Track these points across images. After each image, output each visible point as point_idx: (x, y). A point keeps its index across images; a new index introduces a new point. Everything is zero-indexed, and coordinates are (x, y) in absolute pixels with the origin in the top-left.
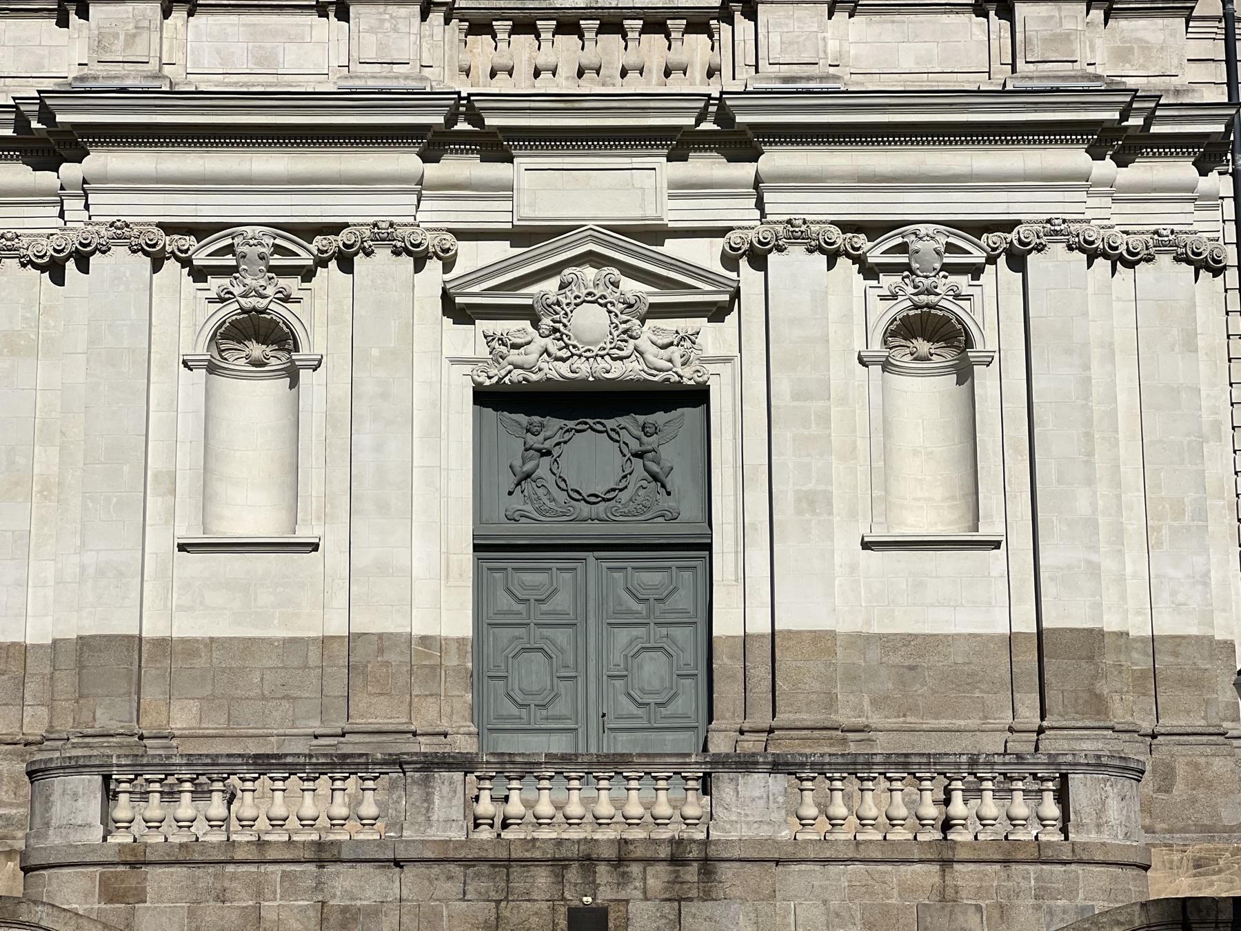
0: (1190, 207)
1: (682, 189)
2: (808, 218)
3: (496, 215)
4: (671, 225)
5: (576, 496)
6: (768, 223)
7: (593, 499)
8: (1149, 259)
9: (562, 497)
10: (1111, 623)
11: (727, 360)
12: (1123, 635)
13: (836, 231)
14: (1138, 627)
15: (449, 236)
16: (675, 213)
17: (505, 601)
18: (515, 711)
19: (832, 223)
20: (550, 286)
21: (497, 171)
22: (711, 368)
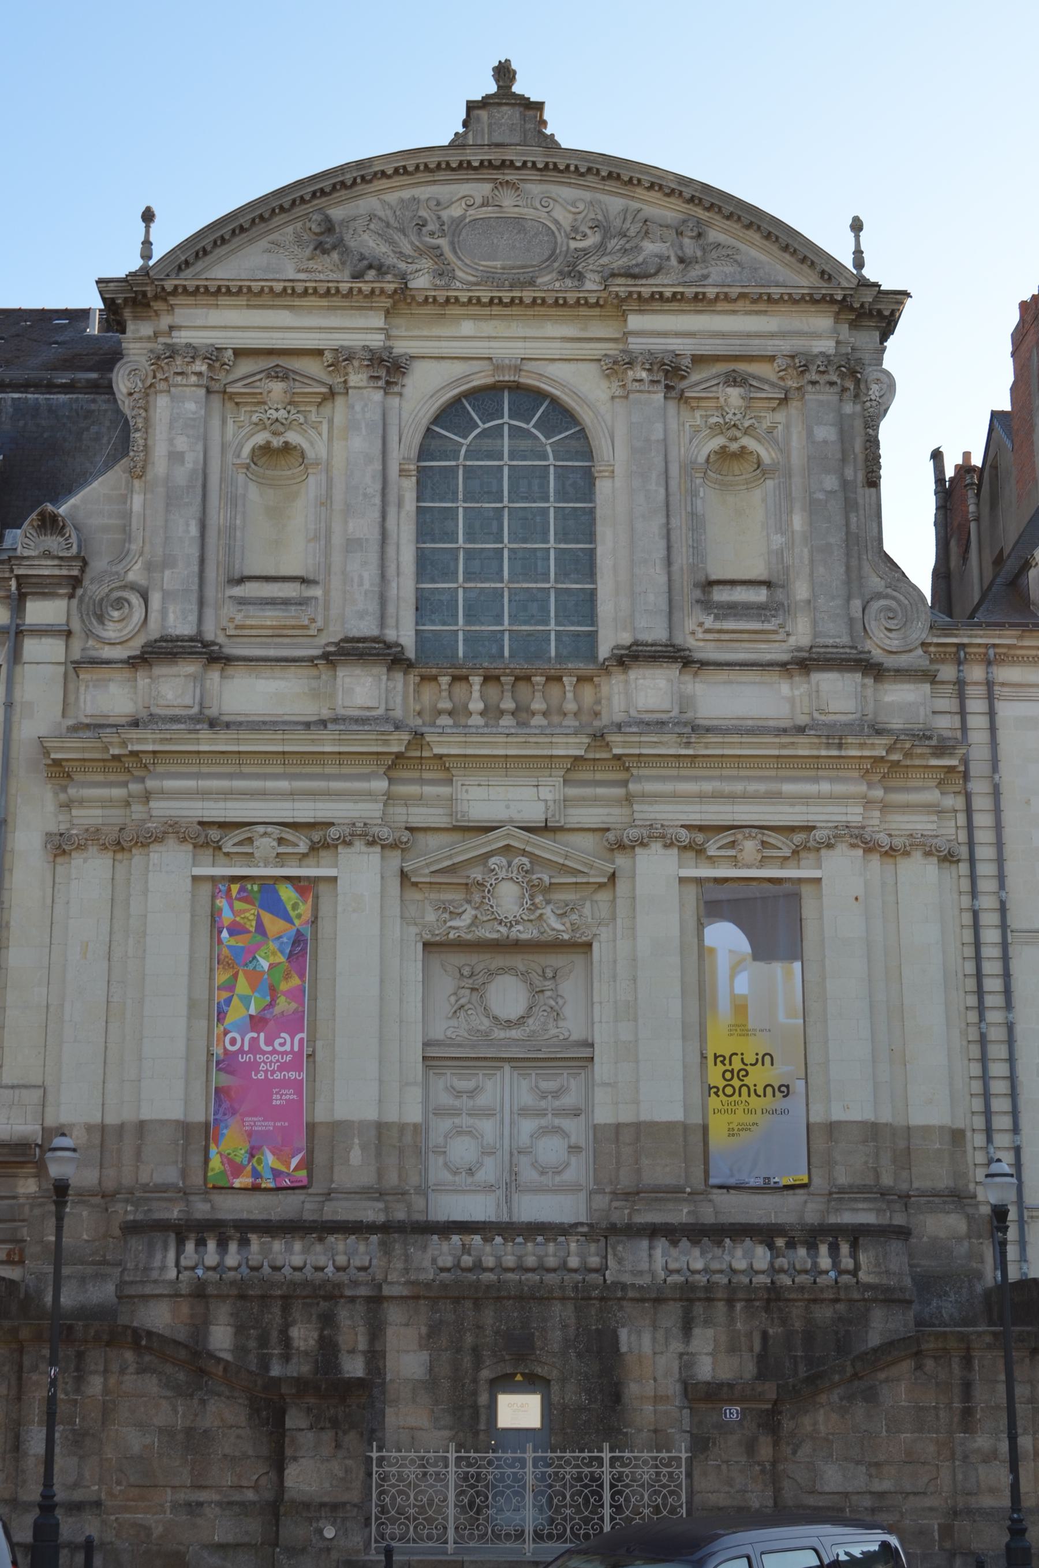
2: (666, 823)
6: (636, 826)
7: (509, 1024)
9: (486, 1022)
13: (683, 831)
18: (448, 1177)
19: (682, 826)
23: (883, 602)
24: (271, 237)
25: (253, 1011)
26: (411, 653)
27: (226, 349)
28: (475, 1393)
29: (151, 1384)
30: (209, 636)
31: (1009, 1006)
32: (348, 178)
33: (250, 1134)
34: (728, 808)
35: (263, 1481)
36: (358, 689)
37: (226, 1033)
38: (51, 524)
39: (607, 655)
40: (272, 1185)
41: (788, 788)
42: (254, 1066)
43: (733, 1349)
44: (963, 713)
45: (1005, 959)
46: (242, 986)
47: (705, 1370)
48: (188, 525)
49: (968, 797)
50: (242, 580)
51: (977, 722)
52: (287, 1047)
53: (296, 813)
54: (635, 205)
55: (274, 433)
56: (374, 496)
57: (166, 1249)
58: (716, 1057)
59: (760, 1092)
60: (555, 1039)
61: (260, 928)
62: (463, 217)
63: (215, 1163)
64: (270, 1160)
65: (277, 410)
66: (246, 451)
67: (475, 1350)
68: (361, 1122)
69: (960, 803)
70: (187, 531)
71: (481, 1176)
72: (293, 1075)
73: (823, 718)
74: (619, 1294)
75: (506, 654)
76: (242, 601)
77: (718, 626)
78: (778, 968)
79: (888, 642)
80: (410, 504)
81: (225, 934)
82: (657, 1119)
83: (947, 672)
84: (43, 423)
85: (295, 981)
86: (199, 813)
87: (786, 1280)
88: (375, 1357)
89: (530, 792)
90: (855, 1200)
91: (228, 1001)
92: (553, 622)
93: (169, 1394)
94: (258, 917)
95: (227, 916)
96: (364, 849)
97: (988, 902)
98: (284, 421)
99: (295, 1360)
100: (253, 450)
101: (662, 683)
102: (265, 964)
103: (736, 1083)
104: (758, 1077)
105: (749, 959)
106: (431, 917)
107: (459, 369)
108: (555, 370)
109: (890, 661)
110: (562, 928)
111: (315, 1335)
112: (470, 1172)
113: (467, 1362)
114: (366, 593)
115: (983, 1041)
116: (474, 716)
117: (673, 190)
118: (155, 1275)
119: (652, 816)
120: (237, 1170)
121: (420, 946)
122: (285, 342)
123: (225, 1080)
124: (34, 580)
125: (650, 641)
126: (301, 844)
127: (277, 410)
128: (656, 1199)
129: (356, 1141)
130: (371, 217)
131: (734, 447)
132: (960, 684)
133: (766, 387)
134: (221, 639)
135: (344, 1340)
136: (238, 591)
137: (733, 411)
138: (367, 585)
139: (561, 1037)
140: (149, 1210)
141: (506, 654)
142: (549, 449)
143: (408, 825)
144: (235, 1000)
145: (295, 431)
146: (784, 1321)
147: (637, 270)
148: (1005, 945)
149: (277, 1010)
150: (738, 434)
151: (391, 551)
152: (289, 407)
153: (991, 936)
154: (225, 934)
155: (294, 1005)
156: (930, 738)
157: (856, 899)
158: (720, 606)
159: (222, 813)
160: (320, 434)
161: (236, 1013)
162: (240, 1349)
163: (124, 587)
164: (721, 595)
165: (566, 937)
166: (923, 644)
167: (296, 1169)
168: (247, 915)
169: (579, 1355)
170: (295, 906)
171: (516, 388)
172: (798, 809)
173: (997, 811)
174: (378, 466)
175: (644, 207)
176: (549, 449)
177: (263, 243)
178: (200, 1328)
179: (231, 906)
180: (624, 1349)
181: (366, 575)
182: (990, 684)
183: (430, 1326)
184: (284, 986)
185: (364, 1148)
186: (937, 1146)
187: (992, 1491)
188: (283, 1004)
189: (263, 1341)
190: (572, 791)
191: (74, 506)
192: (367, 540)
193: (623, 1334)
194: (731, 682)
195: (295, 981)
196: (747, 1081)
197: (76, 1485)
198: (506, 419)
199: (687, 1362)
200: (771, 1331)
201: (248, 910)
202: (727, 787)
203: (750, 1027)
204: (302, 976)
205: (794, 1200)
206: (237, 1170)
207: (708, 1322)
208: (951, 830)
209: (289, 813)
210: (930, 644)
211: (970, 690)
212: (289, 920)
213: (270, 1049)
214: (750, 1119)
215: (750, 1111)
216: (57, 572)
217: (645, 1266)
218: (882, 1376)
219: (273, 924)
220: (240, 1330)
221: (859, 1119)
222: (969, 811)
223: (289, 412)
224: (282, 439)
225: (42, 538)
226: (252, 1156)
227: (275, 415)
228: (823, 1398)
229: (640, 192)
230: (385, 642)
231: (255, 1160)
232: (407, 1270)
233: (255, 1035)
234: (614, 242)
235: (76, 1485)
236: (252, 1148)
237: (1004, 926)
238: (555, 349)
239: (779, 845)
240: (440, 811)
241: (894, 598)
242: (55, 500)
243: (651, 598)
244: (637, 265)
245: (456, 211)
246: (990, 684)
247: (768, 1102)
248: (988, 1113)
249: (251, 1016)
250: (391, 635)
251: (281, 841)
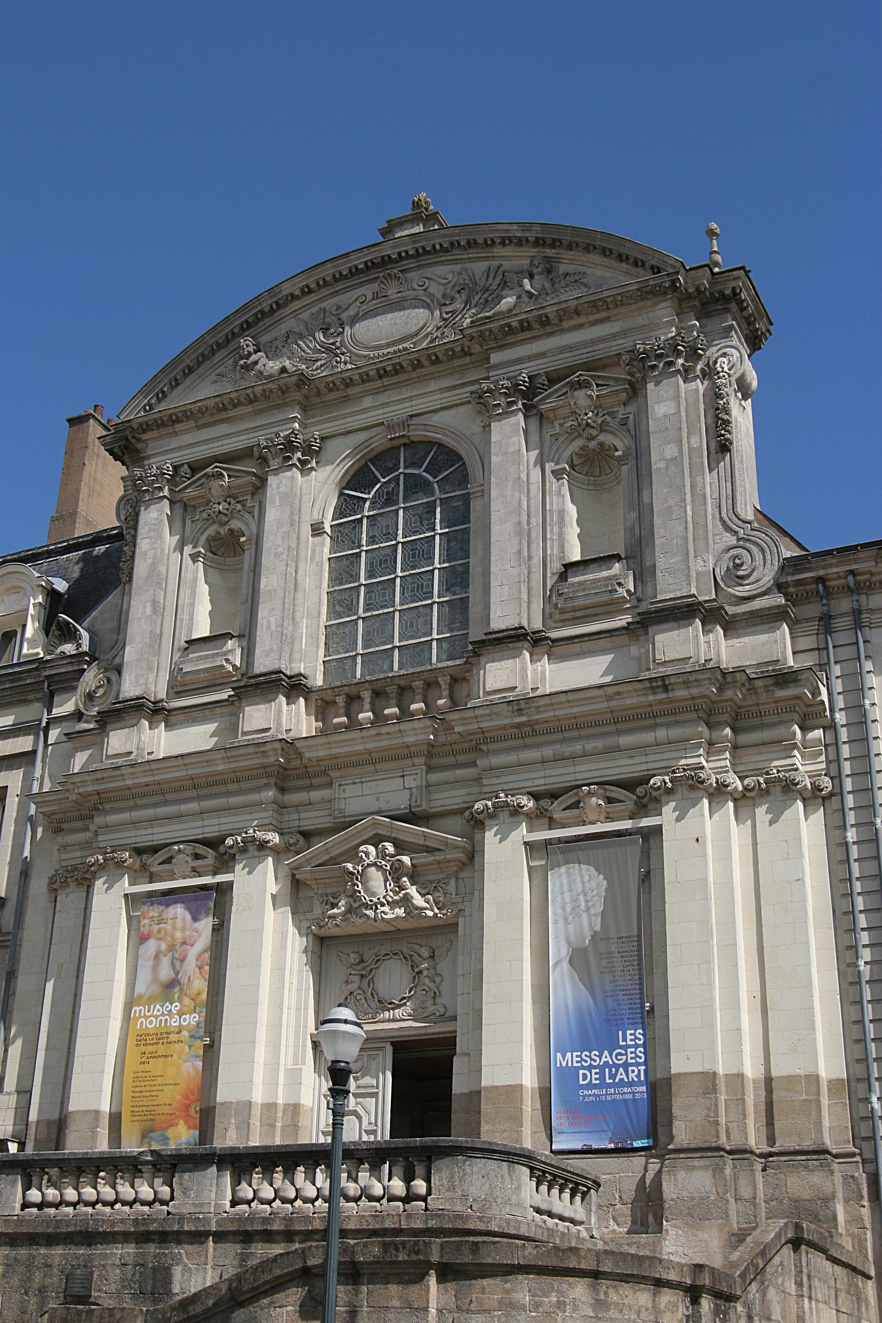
27: (183, 465)
32: (265, 306)
41: (625, 740)
48: (145, 607)
53: (205, 830)
54: (495, 263)
55: (222, 524)
56: (283, 553)
60: (433, 1017)
62: (358, 313)
65: (219, 504)
70: (145, 612)
82: (497, 1083)
86: (133, 840)
89: (397, 783)
96: (256, 853)
98: (225, 512)
100: (208, 539)
107: (362, 437)
114: (272, 635)
117: (520, 239)
122: (223, 448)
124: (56, 679)
125: (504, 628)
126: (210, 856)
131: (593, 444)
133: (611, 382)
137: (584, 411)
138: (273, 627)
139: (438, 1014)
143: (301, 829)
145: (237, 518)
150: (594, 432)
152: (228, 500)
157: (697, 840)
159: (150, 838)
160: (253, 517)
171: (411, 445)
175: (504, 263)
177: (213, 377)
181: (273, 619)
190: (434, 777)
191: (95, 617)
192: (275, 590)
202: (567, 749)
209: (200, 831)
216: (70, 669)
221: (700, 1070)
223: (229, 504)
224: (227, 527)
229: (499, 251)
238: (435, 400)
239: (622, 798)
240: (326, 812)
246: (857, 613)
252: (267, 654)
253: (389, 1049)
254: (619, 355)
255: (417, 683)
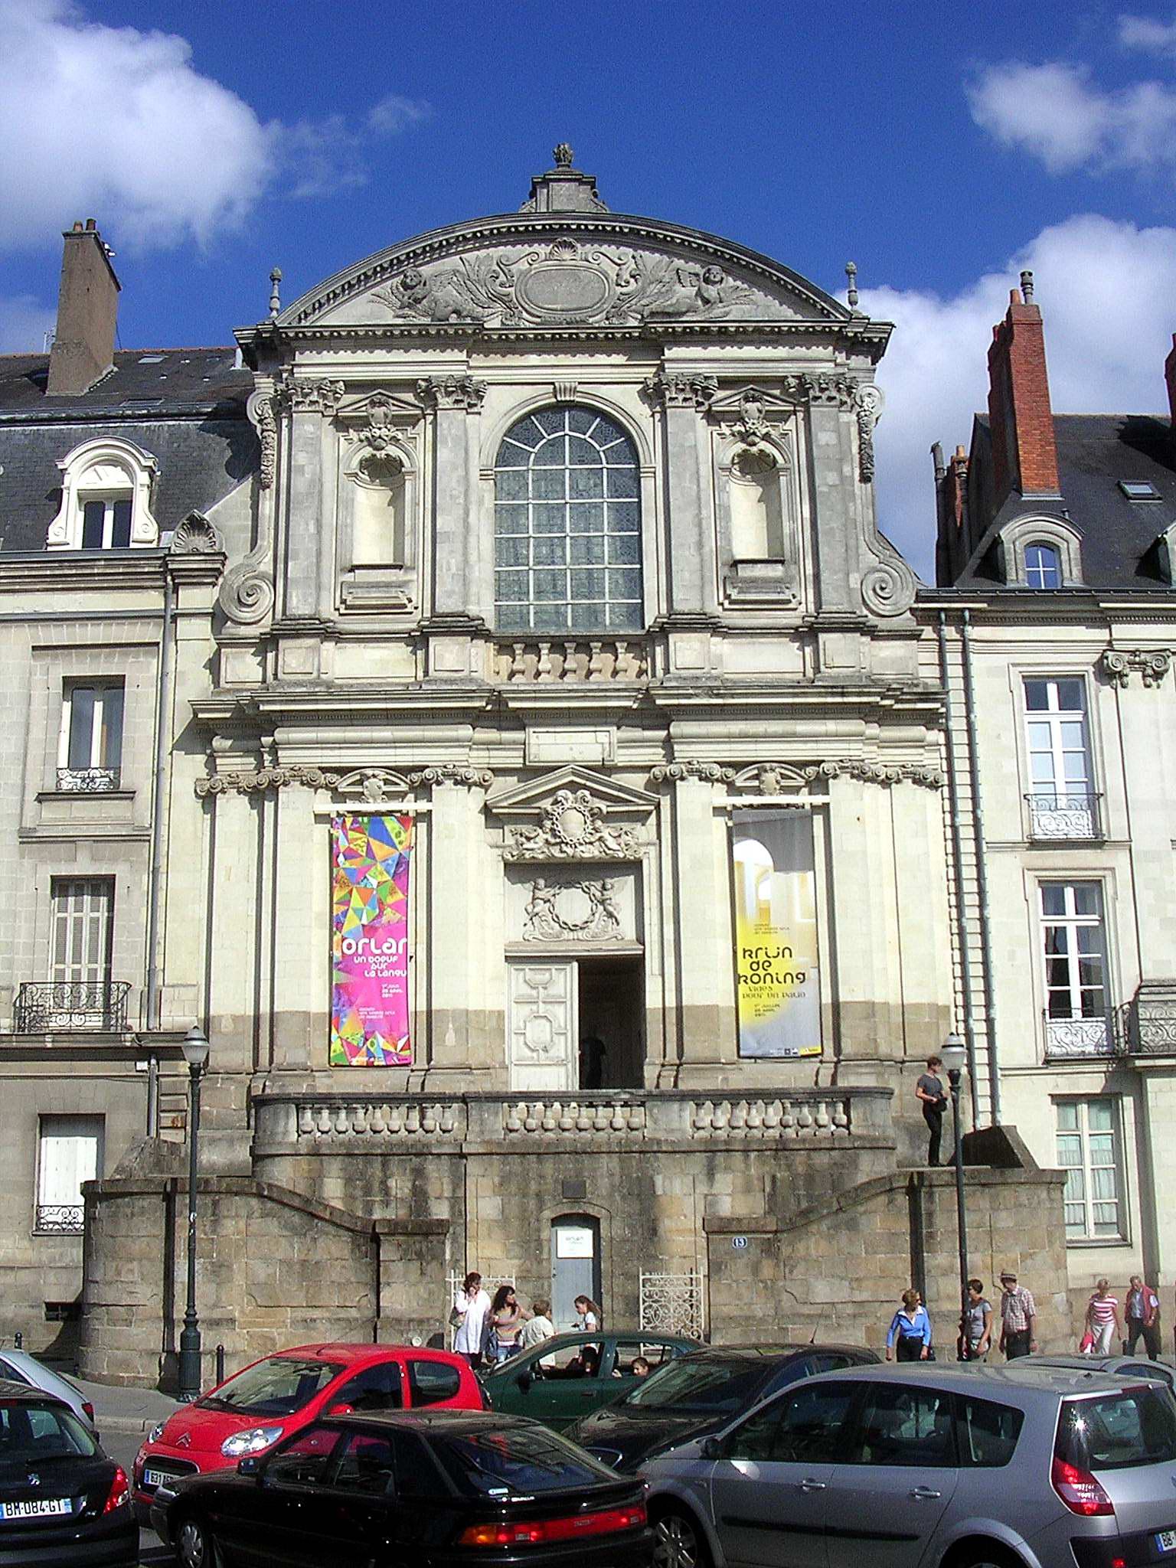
0: (921, 751)
1: (624, 744)
2: (700, 760)
3: (513, 759)
4: (620, 764)
5: (564, 926)
7: (574, 928)
8: (898, 781)
10: (878, 998)
11: (654, 844)
12: (886, 1004)
14: (894, 1000)
15: (490, 773)
16: (622, 758)
17: (525, 990)
18: (529, 1053)
20: (546, 804)
21: (518, 735)
22: (643, 849)
23: (877, 575)
24: (373, 291)
25: (365, 921)
26: (491, 625)
27: (338, 381)
28: (539, 1230)
29: (273, 1226)
30: (325, 616)
31: (982, 906)
33: (364, 1022)
34: (752, 746)
35: (364, 1301)
36: (447, 655)
37: (343, 939)
38: (198, 526)
39: (651, 623)
40: (384, 1063)
42: (366, 966)
43: (748, 1190)
44: (942, 664)
45: (979, 866)
46: (356, 901)
47: (726, 1207)
49: (948, 733)
50: (353, 569)
51: (955, 671)
52: (393, 950)
57: (287, 1117)
58: (745, 951)
59: (781, 979)
61: (370, 853)
63: (336, 1045)
64: (381, 1043)
66: (355, 462)
67: (538, 1195)
68: (454, 1011)
69: (941, 738)
71: (552, 1053)
72: (398, 973)
73: (829, 670)
74: (655, 1148)
75: (570, 623)
76: (353, 585)
77: (742, 597)
78: (795, 876)
79: (882, 607)
80: (489, 502)
81: (341, 859)
83: (928, 632)
84: (193, 444)
85: (400, 896)
86: (319, 760)
87: (790, 1133)
88: (458, 1203)
90: (860, 1066)
91: (345, 914)
92: (607, 595)
93: (287, 1233)
94: (368, 844)
95: (343, 844)
97: (965, 819)
99: (393, 1205)
100: (361, 461)
101: (697, 645)
102: (374, 883)
103: (761, 972)
104: (779, 967)
105: (771, 870)
106: (510, 841)
108: (603, 391)
109: (882, 624)
110: (618, 848)
111: (410, 1185)
112: (545, 1050)
113: (532, 1204)
115: (962, 933)
116: (543, 675)
118: (279, 1138)
119: (691, 754)
120: (355, 1051)
121: (502, 865)
123: (339, 977)
127: (380, 429)
128: (697, 1069)
129: (451, 1026)
130: (455, 272)
132: (941, 641)
134: (335, 616)
135: (433, 1189)
136: (349, 577)
138: (454, 570)
140: (283, 1085)
141: (570, 623)
142: (602, 454)
144: (350, 910)
146: (789, 1167)
147: (671, 310)
148: (978, 854)
149: (384, 920)
150: (757, 440)
151: (472, 540)
153: (968, 847)
154: (341, 859)
155: (398, 916)
156: (917, 686)
158: (745, 580)
161: (352, 923)
162: (349, 1198)
163: (255, 577)
164: (744, 572)
165: (621, 855)
166: (911, 609)
167: (402, 1050)
168: (359, 842)
169: (623, 1197)
170: (398, 835)
172: (810, 746)
173: (971, 744)
174: (461, 472)
176: (602, 454)
177: (368, 295)
178: (316, 1180)
179: (346, 836)
180: (659, 1192)
182: (964, 642)
183: (502, 1177)
184: (390, 900)
185: (456, 1031)
186: (927, 1020)
187: (949, 1298)
188: (390, 915)
189: (367, 1191)
193: (659, 1180)
194: (754, 643)
195: (400, 896)
196: (770, 970)
197: (215, 1306)
198: (567, 431)
199: (710, 1200)
200: (779, 1175)
201: (357, 839)
203: (772, 926)
204: (405, 891)
205: (812, 1066)
206: (355, 1051)
207: (728, 1169)
208: (932, 761)
210: (916, 609)
211: (948, 646)
212: (393, 846)
213: (378, 952)
214: (775, 1001)
215: (773, 995)
216: (203, 566)
217: (675, 1125)
218: (861, 1209)
219: (380, 849)
220: (349, 1181)
221: (863, 999)
222: (949, 745)
225: (192, 538)
226: (366, 1040)
227: (378, 433)
228: (814, 1228)
230: (468, 616)
231: (368, 1043)
232: (482, 1132)
233: (367, 941)
234: (652, 287)
235: (215, 1306)
236: (366, 1033)
237: (977, 839)
241: (886, 572)
242: (203, 508)
243: (687, 575)
244: (671, 305)
245: (524, 266)
246: (964, 642)
247: (788, 987)
248: (966, 992)
249: (363, 925)
250: (473, 610)
251: (386, 782)
252: (449, 594)
253: (575, 965)
254: (786, 377)
255: (595, 644)
